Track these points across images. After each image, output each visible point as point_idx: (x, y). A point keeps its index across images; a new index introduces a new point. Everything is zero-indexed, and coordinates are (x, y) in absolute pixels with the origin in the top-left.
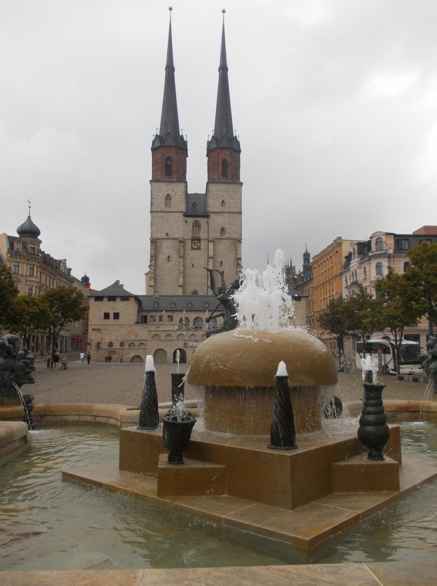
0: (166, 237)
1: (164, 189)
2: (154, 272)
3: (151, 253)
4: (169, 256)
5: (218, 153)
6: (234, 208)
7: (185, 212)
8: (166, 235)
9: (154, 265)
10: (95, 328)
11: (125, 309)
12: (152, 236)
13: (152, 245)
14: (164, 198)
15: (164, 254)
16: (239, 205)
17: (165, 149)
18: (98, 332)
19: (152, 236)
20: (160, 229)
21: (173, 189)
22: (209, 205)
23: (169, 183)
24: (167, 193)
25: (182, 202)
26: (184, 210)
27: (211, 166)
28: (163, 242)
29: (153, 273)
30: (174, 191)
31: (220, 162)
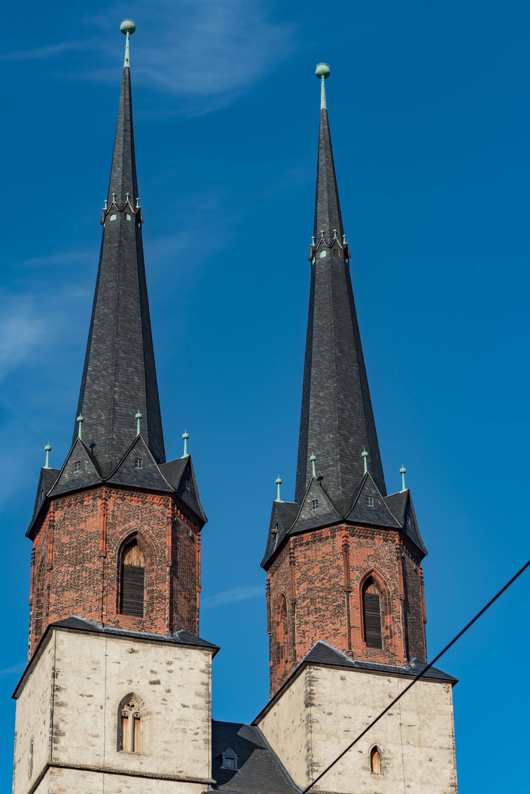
1: (114, 668)
5: (346, 546)
6: (423, 783)
7: (213, 785)
14: (112, 706)
16: (444, 771)
17: (119, 501)
21: (152, 672)
22: (315, 760)
23: (137, 646)
24: (126, 690)
25: (194, 737)
26: (206, 774)
27: (305, 598)
30: (158, 683)
31: (356, 585)
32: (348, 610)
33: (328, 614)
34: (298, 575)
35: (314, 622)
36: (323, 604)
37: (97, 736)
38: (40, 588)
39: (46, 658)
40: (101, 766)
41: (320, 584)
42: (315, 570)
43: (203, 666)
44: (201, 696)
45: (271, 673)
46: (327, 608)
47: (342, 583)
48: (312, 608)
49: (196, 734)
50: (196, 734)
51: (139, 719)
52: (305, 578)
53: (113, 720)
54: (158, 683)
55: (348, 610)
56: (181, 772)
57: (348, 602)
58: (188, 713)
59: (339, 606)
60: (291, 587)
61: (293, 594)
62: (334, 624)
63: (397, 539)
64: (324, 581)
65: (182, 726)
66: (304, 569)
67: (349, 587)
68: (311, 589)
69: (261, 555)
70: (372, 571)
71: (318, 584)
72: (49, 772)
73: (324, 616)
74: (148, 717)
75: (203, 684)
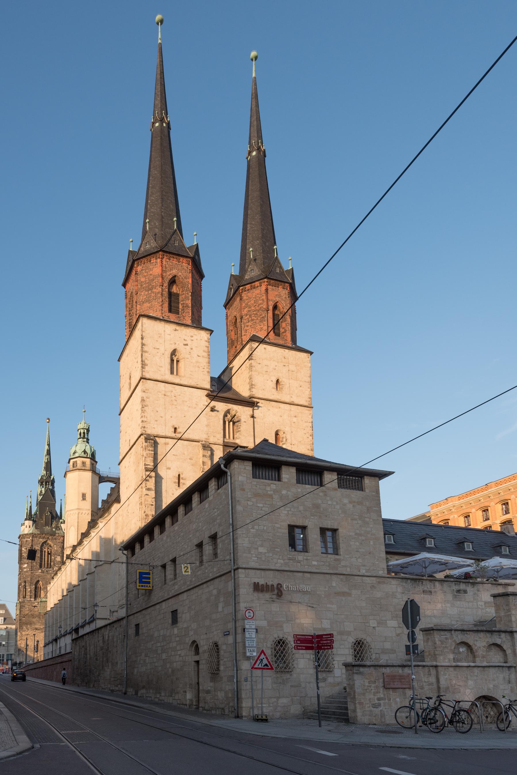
0: (173, 435)
2: (154, 504)
3: (147, 463)
4: (179, 475)
8: (173, 430)
9: (153, 488)
10: (262, 582)
11: (355, 519)
12: (145, 429)
13: (148, 446)
15: (169, 468)
18: (274, 597)
19: (145, 429)
20: (161, 417)
25: (203, 370)
27: (246, 315)
28: (168, 444)
29: (152, 505)
30: (187, 345)
31: (271, 308)
32: (267, 319)
33: (258, 321)
34: (244, 305)
35: (251, 325)
36: (255, 317)
37: (162, 367)
38: (130, 307)
39: (137, 333)
40: (164, 380)
41: (254, 308)
42: (252, 302)
43: (206, 339)
44: (205, 352)
45: (228, 353)
46: (257, 319)
47: (265, 307)
48: (250, 319)
49: (204, 368)
50: (204, 368)
51: (179, 361)
52: (247, 306)
53: (168, 360)
54: (187, 345)
55: (267, 319)
56: (198, 385)
57: (267, 315)
58: (200, 359)
59: (263, 317)
60: (240, 310)
61: (241, 313)
62: (260, 325)
63: (288, 288)
64: (256, 307)
65: (198, 365)
66: (246, 302)
67: (268, 308)
68: (250, 311)
69: (223, 300)
70: (277, 302)
71: (253, 308)
72: (141, 382)
73: (256, 322)
74: (183, 360)
75: (206, 347)
